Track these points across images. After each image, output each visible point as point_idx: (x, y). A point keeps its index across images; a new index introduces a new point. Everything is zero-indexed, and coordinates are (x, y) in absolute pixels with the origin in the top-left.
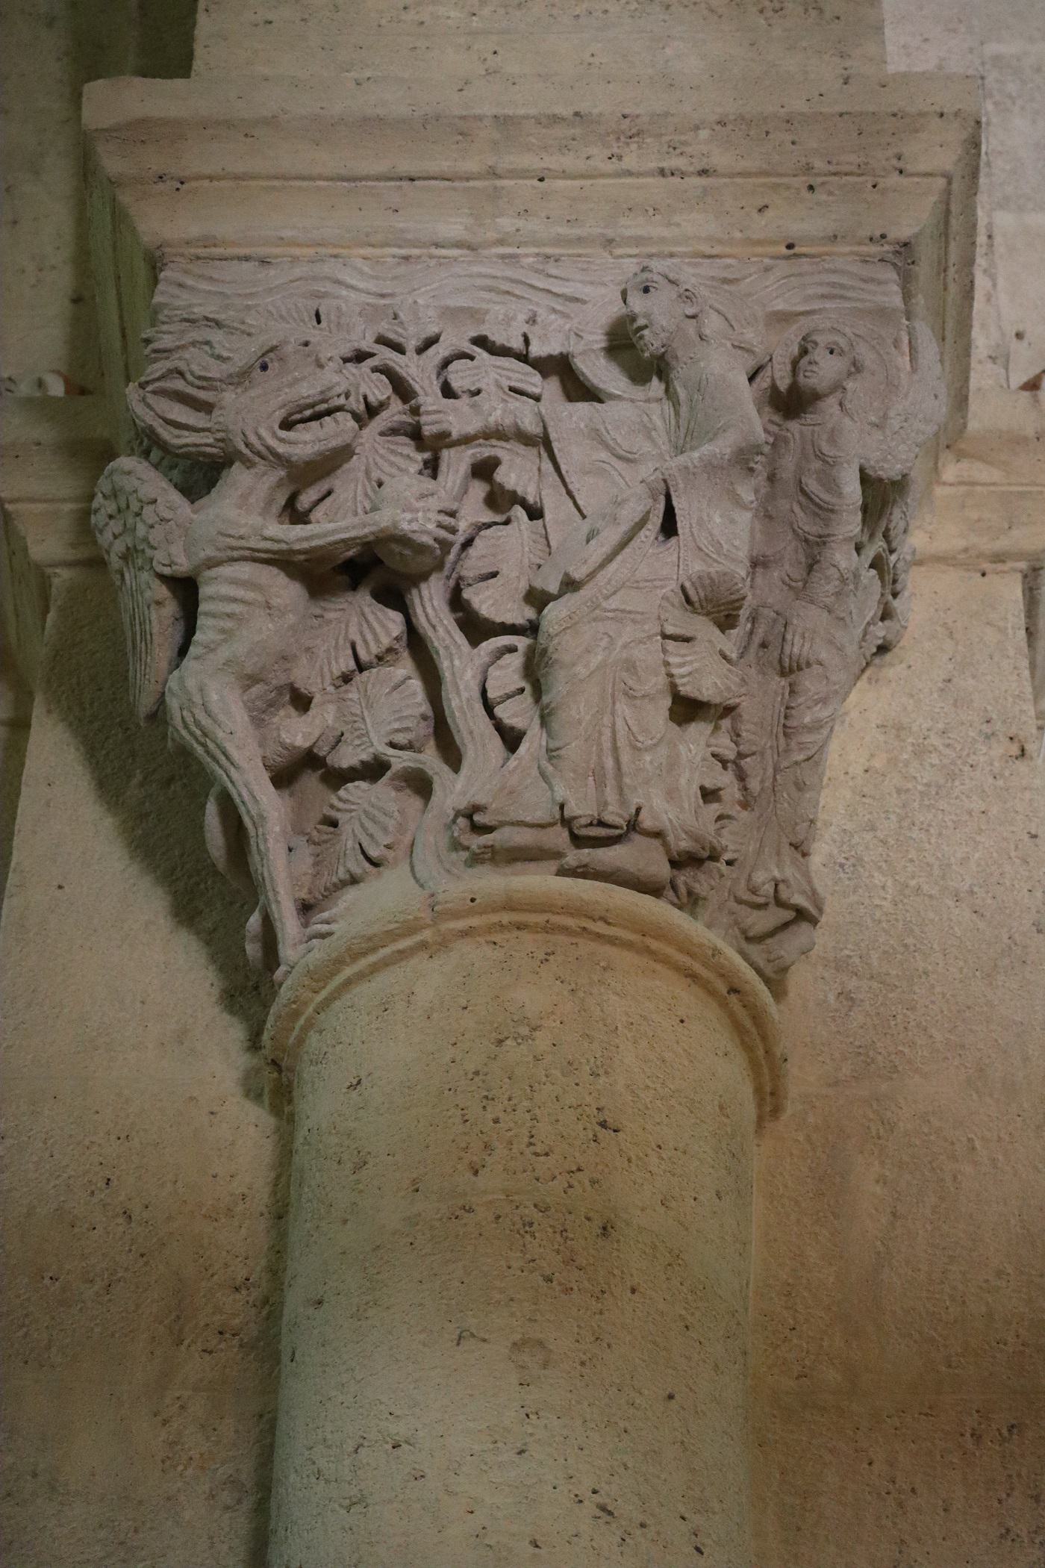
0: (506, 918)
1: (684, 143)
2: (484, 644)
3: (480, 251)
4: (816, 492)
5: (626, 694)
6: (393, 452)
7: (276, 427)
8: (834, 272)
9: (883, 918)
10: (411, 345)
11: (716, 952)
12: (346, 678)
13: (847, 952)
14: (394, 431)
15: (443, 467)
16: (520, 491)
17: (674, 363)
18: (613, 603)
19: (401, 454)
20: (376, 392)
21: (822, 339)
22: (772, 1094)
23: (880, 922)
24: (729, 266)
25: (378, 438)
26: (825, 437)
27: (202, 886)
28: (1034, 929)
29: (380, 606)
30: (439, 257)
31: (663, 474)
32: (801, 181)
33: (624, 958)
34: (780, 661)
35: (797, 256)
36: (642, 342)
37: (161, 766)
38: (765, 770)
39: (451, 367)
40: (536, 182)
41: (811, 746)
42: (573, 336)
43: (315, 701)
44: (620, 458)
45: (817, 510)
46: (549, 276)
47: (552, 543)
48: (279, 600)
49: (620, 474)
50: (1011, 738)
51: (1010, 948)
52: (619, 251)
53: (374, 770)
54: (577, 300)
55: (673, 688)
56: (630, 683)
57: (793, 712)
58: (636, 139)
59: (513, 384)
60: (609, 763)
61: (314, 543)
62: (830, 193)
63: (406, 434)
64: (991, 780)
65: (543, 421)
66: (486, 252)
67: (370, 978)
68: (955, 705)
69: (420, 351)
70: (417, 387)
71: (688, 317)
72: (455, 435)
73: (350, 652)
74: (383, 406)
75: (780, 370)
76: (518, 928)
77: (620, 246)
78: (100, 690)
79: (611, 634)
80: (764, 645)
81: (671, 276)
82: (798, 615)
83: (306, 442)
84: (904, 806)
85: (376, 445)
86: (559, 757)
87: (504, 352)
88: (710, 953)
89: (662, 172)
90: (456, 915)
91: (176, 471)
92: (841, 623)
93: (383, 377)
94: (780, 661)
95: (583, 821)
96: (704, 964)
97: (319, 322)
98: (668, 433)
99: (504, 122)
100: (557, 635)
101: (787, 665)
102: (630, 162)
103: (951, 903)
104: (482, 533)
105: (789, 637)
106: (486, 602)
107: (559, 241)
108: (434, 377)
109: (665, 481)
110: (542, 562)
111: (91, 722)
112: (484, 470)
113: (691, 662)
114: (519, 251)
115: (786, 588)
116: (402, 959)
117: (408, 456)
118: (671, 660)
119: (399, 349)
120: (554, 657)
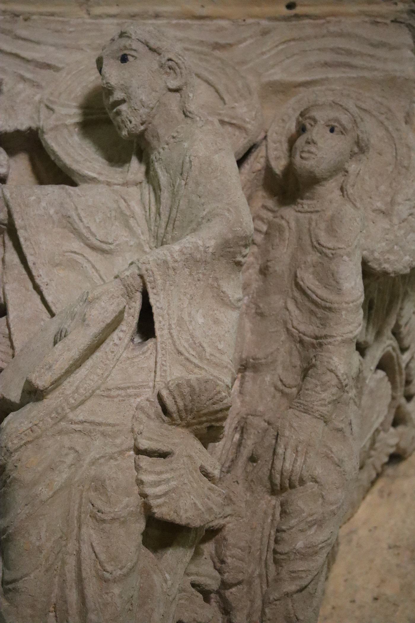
4: (312, 287)
5: (94, 517)
8: (340, 35)
17: (154, 143)
18: (80, 414)
21: (320, 115)
24: (220, 29)
26: (323, 225)
31: (139, 269)
34: (271, 478)
35: (297, 17)
36: (119, 119)
38: (252, 601)
41: (304, 575)
42: (44, 110)
44: (93, 248)
45: (313, 308)
46: (18, 38)
47: (15, 344)
49: (93, 267)
52: (97, 10)
54: (48, 66)
55: (147, 508)
56: (99, 504)
57: (284, 535)
60: (73, 596)
65: (8, 206)
71: (170, 90)
75: (276, 149)
79: (78, 448)
80: (253, 459)
81: (153, 43)
82: (291, 426)
86: (15, 590)
92: (339, 435)
94: (271, 478)
98: (148, 221)
100: (16, 450)
101: (278, 481)
105: (280, 451)
109: (141, 277)
113: (167, 481)
115: (278, 395)
118: (145, 478)
120: (14, 475)
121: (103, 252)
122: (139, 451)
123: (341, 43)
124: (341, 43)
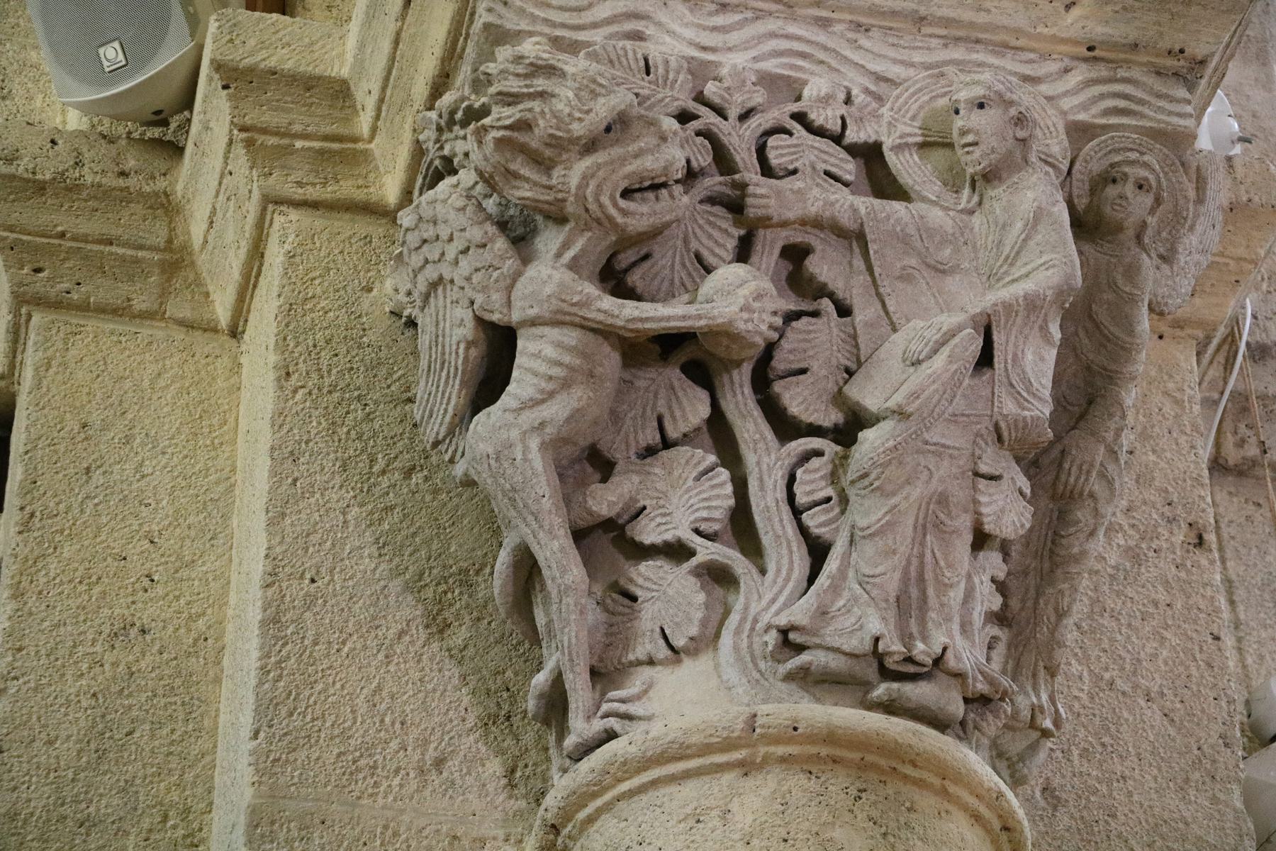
0: (825, 751)
2: (794, 444)
3: (795, 9)
4: (1106, 324)
6: (710, 223)
7: (618, 195)
9: (1082, 711)
10: (733, 113)
11: (1000, 795)
12: (650, 452)
14: (711, 200)
16: (831, 286)
19: (720, 228)
23: (1079, 715)
25: (699, 207)
26: (1121, 269)
27: (449, 595)
28: (1221, 741)
29: (690, 383)
30: (755, 9)
35: (1095, 59)
37: (401, 452)
39: (772, 141)
43: (618, 468)
46: (860, 47)
50: (1190, 524)
51: (1200, 761)
52: (927, 30)
53: (677, 552)
59: (829, 168)
61: (648, 326)
63: (721, 204)
64: (1173, 569)
67: (682, 782)
72: (775, 220)
73: (655, 424)
74: (702, 172)
76: (834, 761)
77: (930, 24)
79: (930, 467)
82: (1078, 446)
83: (641, 216)
84: (1096, 589)
85: (695, 213)
87: (819, 132)
88: (995, 796)
90: (777, 740)
92: (1114, 455)
93: (706, 142)
95: (896, 658)
96: (989, 806)
97: (648, 73)
103: (1142, 703)
105: (1066, 466)
111: (330, 392)
112: (795, 255)
116: (717, 772)
117: (726, 230)
119: (721, 112)
121: (937, 270)
122: (977, 474)
123: (1128, 89)
124: (1128, 89)
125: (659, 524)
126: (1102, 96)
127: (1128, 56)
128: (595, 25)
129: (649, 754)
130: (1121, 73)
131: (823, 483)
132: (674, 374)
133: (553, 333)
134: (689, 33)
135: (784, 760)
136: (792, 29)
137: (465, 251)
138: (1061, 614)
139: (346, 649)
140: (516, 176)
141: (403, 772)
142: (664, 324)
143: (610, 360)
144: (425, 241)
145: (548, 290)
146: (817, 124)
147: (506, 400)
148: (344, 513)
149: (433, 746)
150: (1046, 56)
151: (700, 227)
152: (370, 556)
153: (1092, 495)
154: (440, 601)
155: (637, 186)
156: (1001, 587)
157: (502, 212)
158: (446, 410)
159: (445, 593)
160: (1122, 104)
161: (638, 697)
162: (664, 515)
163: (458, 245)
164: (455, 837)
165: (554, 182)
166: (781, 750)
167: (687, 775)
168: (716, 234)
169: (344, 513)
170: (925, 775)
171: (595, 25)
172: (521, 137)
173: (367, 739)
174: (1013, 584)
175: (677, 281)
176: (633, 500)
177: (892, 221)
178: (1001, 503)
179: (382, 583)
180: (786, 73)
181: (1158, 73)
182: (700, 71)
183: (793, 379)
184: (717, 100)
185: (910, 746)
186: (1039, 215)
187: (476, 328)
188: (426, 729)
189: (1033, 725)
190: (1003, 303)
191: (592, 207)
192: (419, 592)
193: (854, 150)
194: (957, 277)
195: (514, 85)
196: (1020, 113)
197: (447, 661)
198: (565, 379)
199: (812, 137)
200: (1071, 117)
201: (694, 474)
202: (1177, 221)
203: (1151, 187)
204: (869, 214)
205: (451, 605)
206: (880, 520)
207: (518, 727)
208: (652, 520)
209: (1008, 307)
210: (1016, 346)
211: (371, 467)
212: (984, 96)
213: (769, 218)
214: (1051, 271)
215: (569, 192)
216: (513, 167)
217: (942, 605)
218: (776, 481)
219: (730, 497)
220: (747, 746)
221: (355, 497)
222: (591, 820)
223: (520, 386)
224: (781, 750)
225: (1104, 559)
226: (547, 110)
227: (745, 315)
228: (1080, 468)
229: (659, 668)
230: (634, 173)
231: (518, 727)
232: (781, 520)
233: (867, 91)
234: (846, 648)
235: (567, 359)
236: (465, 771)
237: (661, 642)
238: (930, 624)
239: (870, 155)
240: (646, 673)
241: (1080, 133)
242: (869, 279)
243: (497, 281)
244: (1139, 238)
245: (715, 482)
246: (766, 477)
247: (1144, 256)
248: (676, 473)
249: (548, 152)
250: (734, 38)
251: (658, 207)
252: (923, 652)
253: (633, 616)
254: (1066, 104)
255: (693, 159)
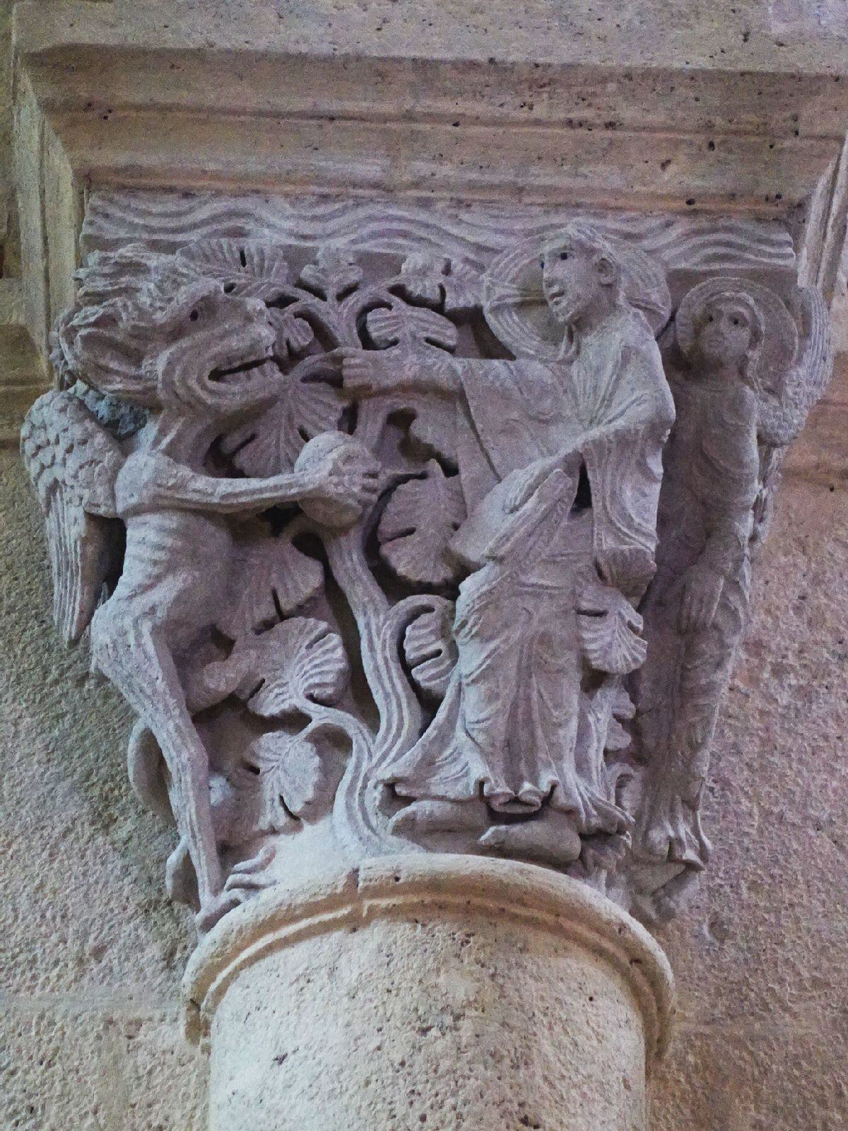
1: (594, 94)
2: (402, 603)
7: (206, 378)
9: (751, 846)
10: (331, 292)
11: (623, 927)
12: (267, 625)
13: (718, 881)
15: (362, 415)
16: (437, 447)
19: (322, 402)
20: (300, 339)
22: (659, 1041)
26: (726, 404)
27: (116, 792)
29: (302, 555)
32: (701, 139)
33: (543, 940)
37: (75, 662)
39: (370, 316)
40: (450, 128)
43: (237, 643)
48: (205, 549)
52: (527, 200)
53: (293, 721)
58: (547, 89)
61: (243, 499)
62: (730, 151)
66: (401, 195)
68: (810, 623)
69: (341, 297)
70: (338, 335)
73: (270, 598)
77: (529, 194)
78: (16, 579)
83: (234, 394)
89: (570, 123)
91: (103, 403)
93: (307, 324)
95: (502, 800)
96: (611, 940)
97: (244, 264)
99: (421, 65)
101: (684, 627)
102: (540, 111)
103: (812, 832)
104: (400, 487)
106: (403, 560)
107: (472, 186)
108: (353, 324)
110: (458, 521)
112: (401, 420)
114: (432, 195)
121: (541, 421)
122: (580, 612)
125: (277, 696)
126: (704, 246)
127: (725, 206)
128: (195, 226)
129: (261, 919)
130: (722, 222)
131: (433, 638)
132: (285, 547)
133: (154, 519)
134: (288, 225)
135: (392, 913)
136: (392, 211)
137: (69, 450)
138: (695, 747)
139: (10, 852)
140: (108, 371)
141: (61, 964)
142: (256, 497)
143: (216, 539)
144: (39, 448)
145: (145, 476)
146: (419, 297)
147: (121, 590)
148: (16, 725)
149: (92, 936)
150: (647, 214)
151: (303, 403)
152: (39, 762)
153: (715, 627)
154: (107, 797)
155: (227, 368)
156: (632, 726)
157: (114, 415)
158: (74, 608)
159: (112, 790)
160: (722, 250)
161: (262, 867)
162: (280, 686)
163: (63, 445)
164: (111, 1022)
165: (142, 371)
166: (384, 903)
167: (299, 937)
168: (319, 408)
169: (16, 725)
170: (536, 914)
171: (195, 226)
172: (106, 333)
173: (28, 935)
174: (645, 721)
175: (282, 456)
176: (251, 675)
177: (491, 378)
178: (608, 639)
179: (50, 786)
180: (384, 251)
181: (759, 220)
182: (295, 258)
183: (402, 540)
184: (313, 282)
185: (516, 885)
186: (627, 355)
187: (88, 523)
188: (87, 920)
189: (671, 858)
190: (594, 441)
191: (181, 391)
192: (86, 791)
193: (457, 317)
194: (561, 425)
195: (100, 285)
196: (603, 259)
197: (111, 854)
198: (169, 561)
199: (411, 308)
200: (673, 267)
201: (307, 642)
202: (782, 356)
203: (745, 319)
204: (465, 373)
205: (117, 801)
206: (481, 665)
207: (179, 911)
208: (271, 691)
209: (598, 444)
210: (613, 483)
211: (45, 678)
212: (565, 247)
213: (369, 387)
214: (643, 406)
215: (157, 379)
216: (102, 362)
217: (552, 745)
218: (385, 641)
219: (341, 661)
220: (351, 901)
221: (27, 708)
222: (221, 991)
223: (133, 572)
224: (384, 903)
225: (776, 700)
226: (129, 303)
227: (335, 479)
228: (701, 601)
229: (282, 836)
230: (220, 354)
231: (179, 911)
232: (390, 678)
233: (466, 260)
234: (452, 795)
235: (169, 542)
236: (123, 958)
237: (281, 810)
238: (539, 764)
239: (471, 320)
240: (272, 841)
241: (680, 281)
242: (473, 435)
243: (99, 475)
244: (741, 372)
245: (327, 647)
246: (375, 639)
247: (747, 389)
248: (291, 643)
249: (133, 344)
250: (332, 225)
251: (249, 385)
252: (529, 792)
253: (256, 787)
254: (667, 255)
255: (292, 340)
